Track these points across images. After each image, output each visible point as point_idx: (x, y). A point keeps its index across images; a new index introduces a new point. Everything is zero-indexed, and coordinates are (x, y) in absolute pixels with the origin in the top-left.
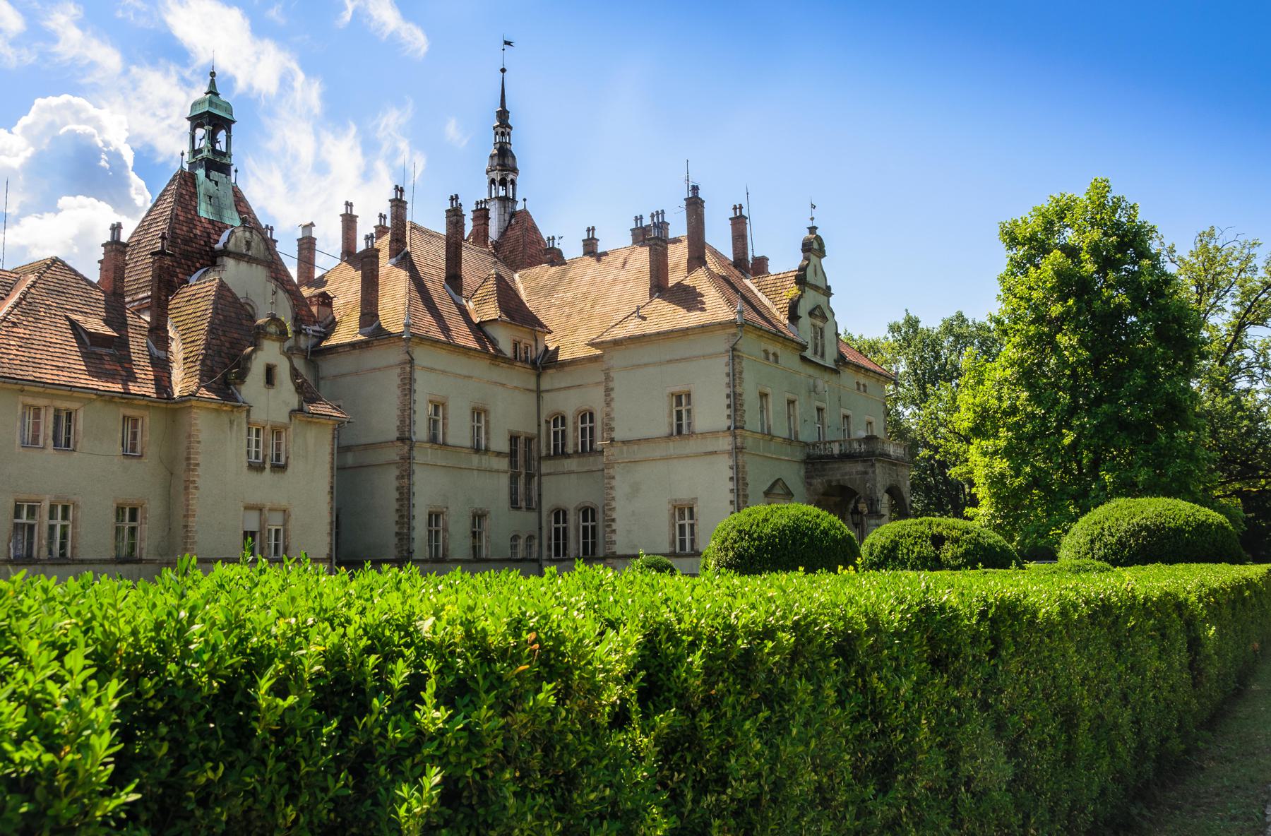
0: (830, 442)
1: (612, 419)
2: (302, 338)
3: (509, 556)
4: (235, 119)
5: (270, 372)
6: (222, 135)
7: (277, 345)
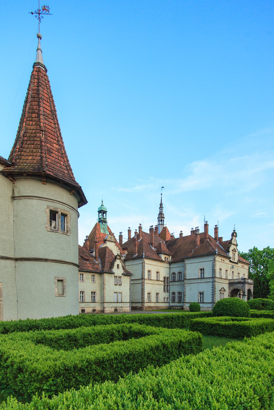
0: (235, 279)
1: (186, 274)
5: (118, 265)
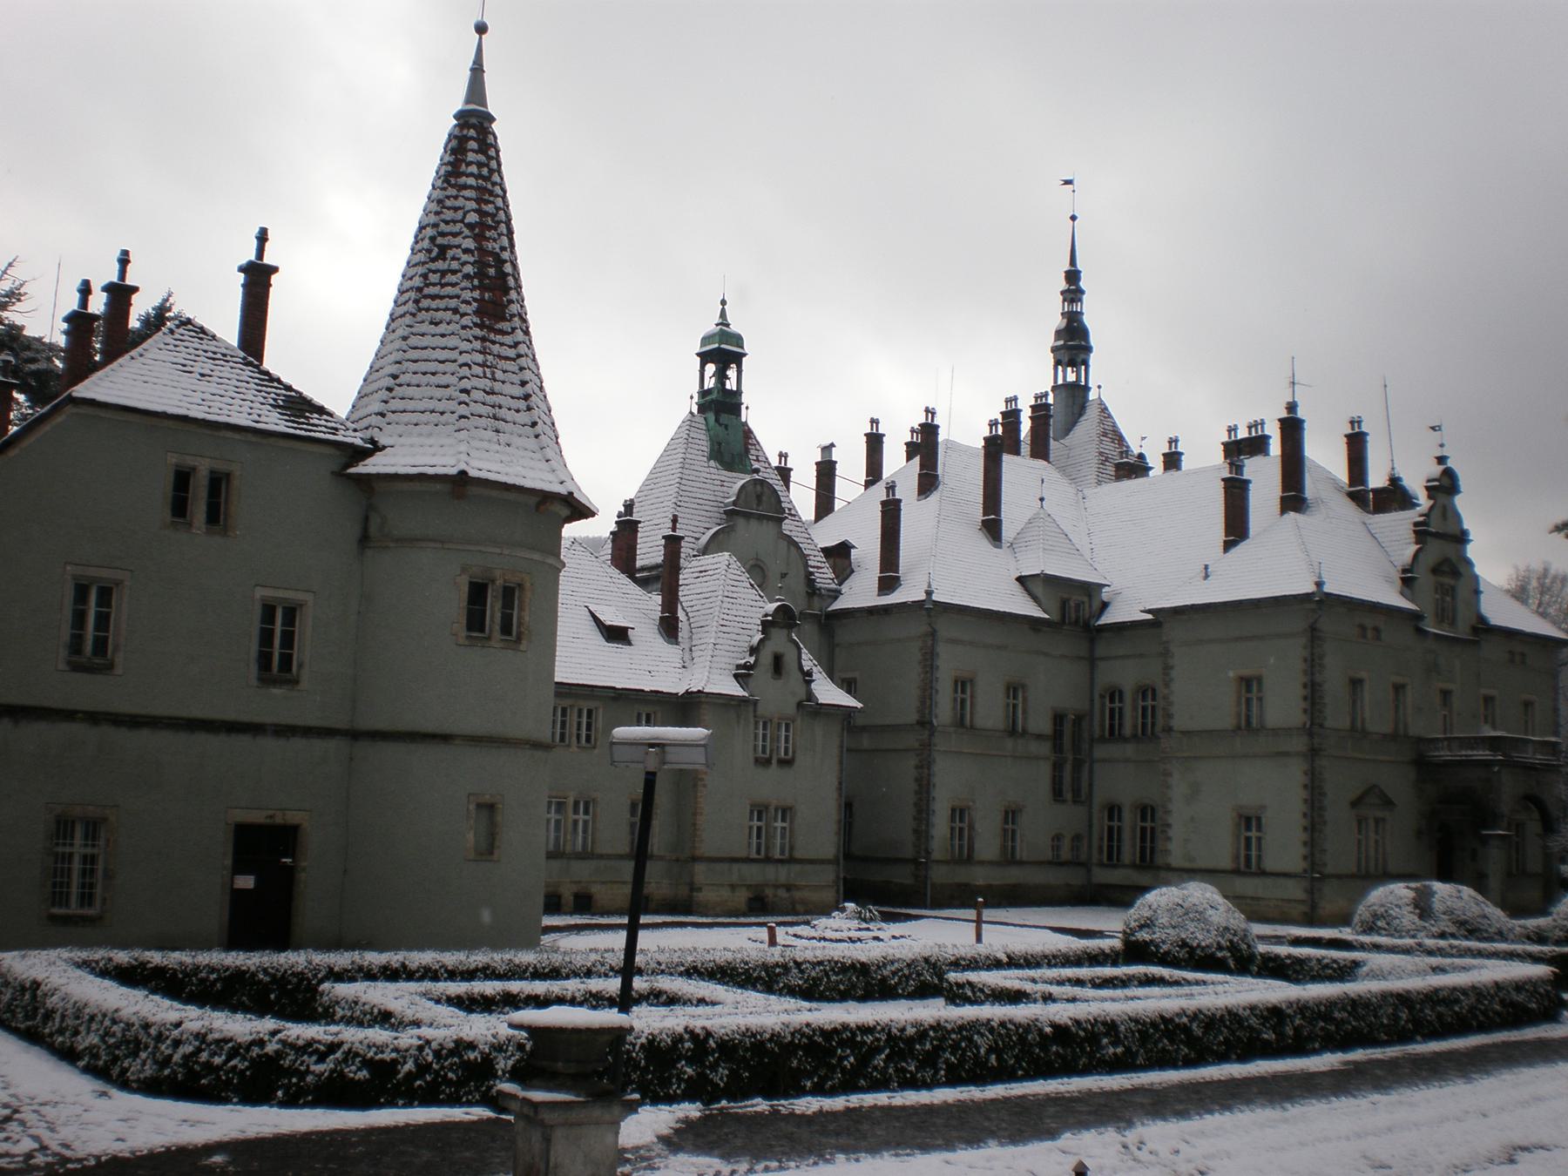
1: (1171, 704)
2: (816, 599)
3: (1048, 855)
4: (747, 351)
6: (732, 373)
7: (785, 631)
